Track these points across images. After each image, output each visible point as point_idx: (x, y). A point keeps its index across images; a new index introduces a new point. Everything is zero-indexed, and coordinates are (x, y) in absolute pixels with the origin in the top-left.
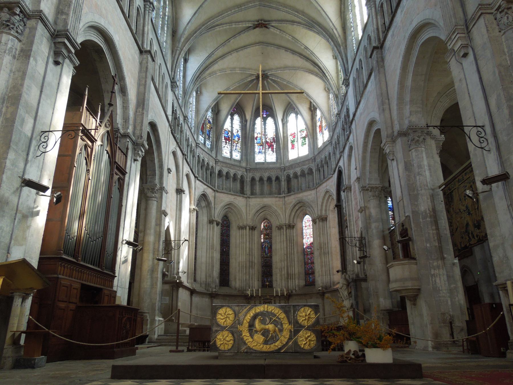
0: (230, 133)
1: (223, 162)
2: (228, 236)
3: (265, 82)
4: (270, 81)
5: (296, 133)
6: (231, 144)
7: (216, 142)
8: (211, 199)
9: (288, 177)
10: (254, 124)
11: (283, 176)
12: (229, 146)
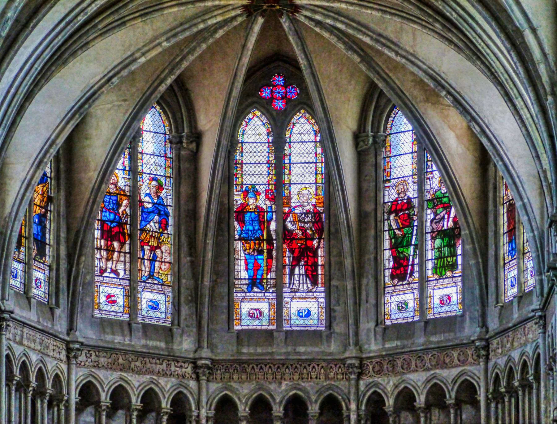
0: (125, 202)
1: (98, 349)
4: (302, 19)
5: (415, 202)
6: (132, 253)
7: (70, 257)
11: (352, 397)
12: (120, 267)
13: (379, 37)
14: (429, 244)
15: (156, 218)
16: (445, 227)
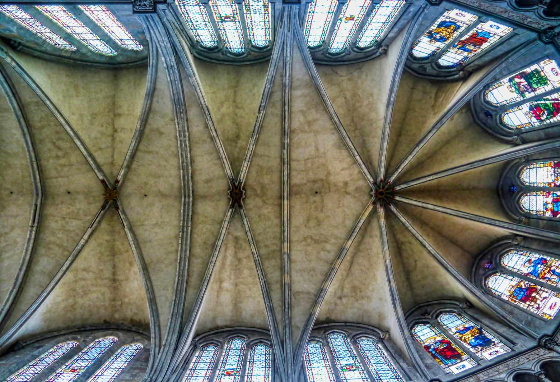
3: (398, 188)
6: (542, 285)
12: (544, 295)
14: (538, 92)
15: (539, 266)
16: (526, 83)
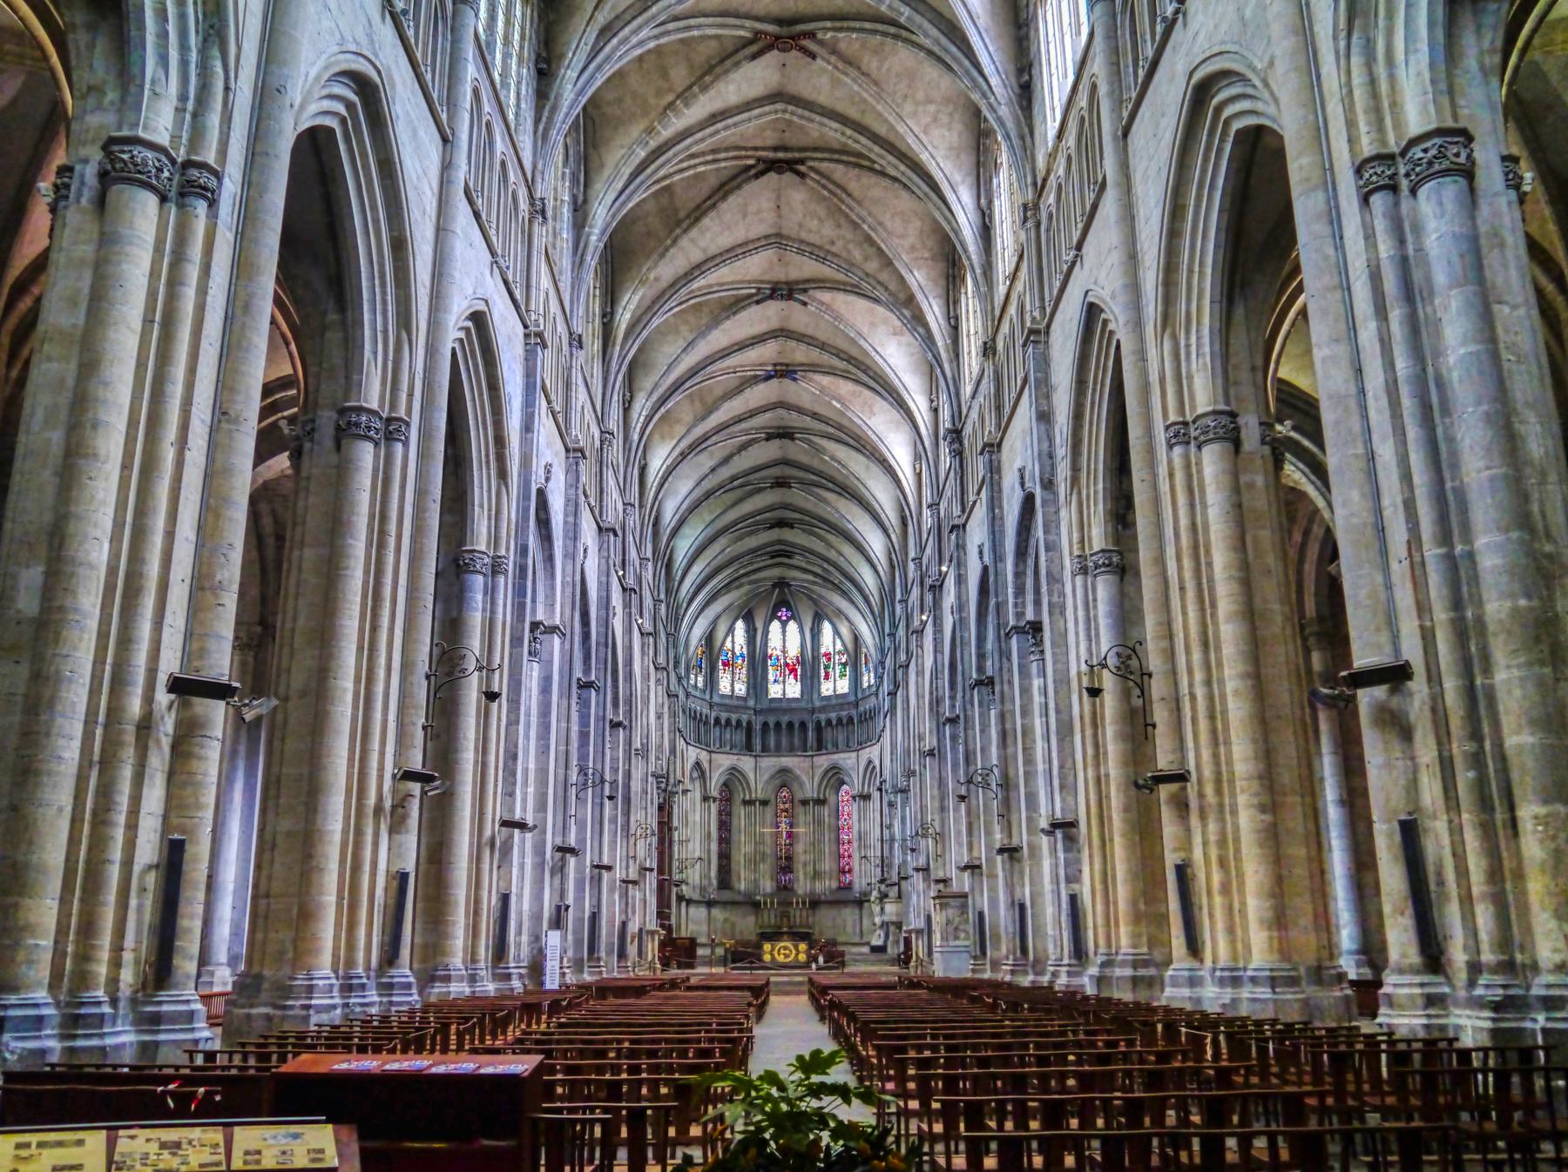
2: (729, 814)
8: (706, 765)
9: (819, 723)
10: (766, 632)
13: (821, 596)
